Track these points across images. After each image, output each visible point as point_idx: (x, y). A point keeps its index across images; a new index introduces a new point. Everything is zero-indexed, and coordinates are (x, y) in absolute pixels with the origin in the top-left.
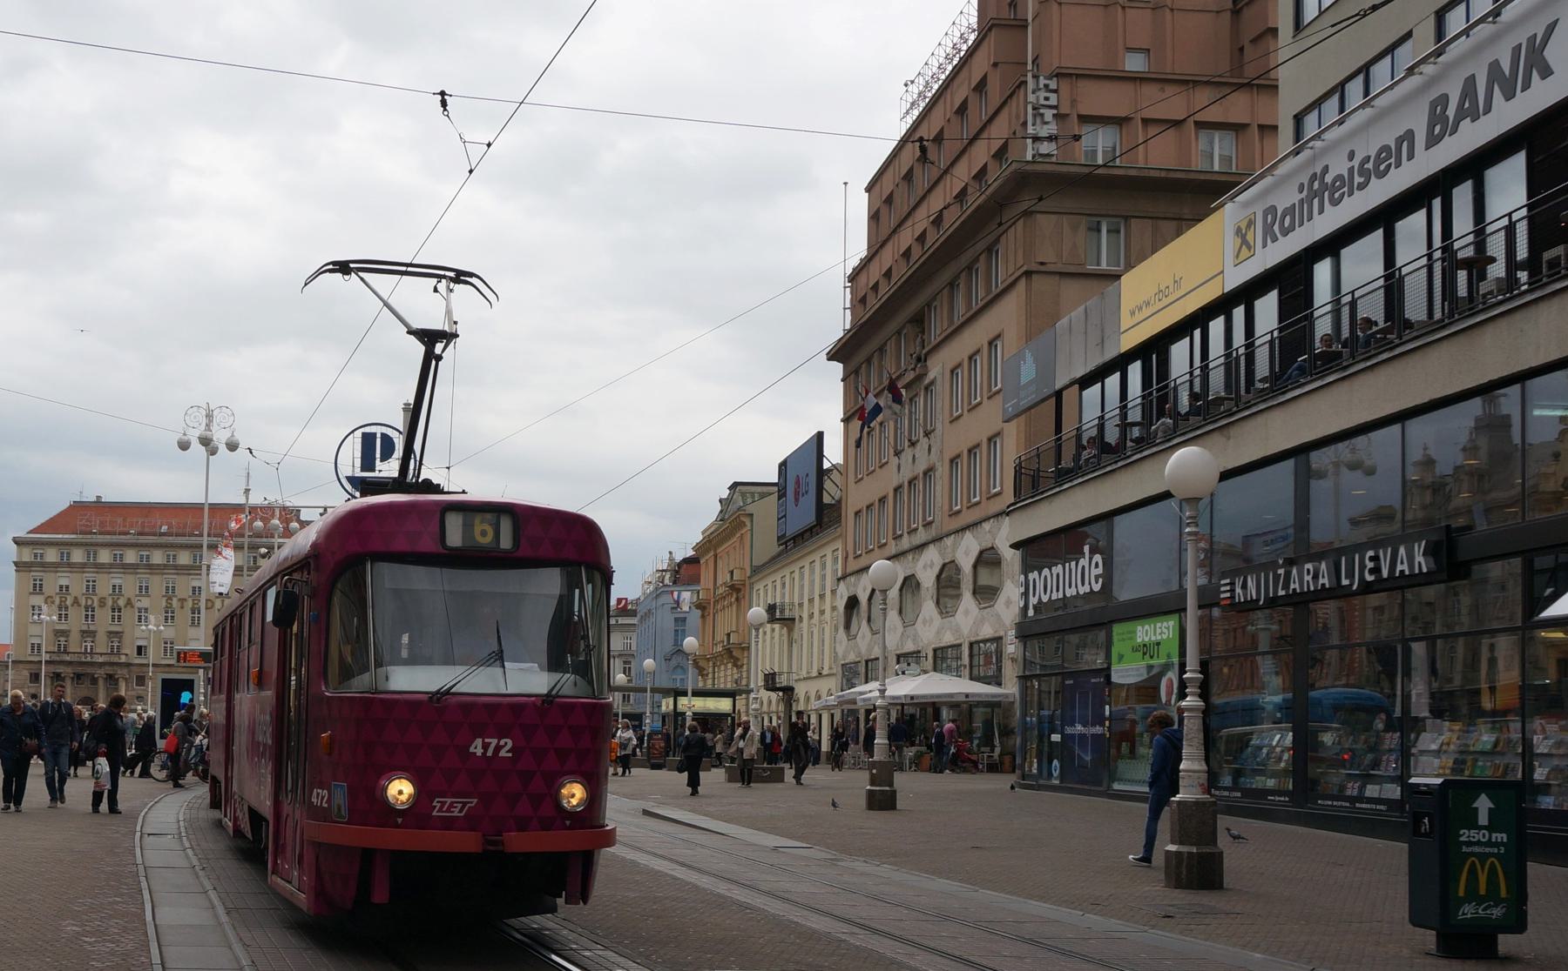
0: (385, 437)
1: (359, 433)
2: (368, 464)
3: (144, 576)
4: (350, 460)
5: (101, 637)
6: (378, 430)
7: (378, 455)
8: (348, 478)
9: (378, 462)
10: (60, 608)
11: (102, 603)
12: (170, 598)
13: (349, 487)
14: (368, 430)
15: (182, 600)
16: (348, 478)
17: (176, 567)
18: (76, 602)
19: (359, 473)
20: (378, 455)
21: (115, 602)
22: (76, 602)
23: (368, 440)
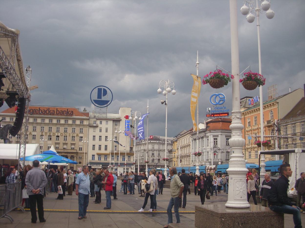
0: (104, 89)
1: (97, 88)
2: (99, 96)
3: (35, 125)
4: (95, 96)
7: (102, 95)
9: (102, 97)
10: (65, 136)
12: (42, 132)
14: (100, 87)
15: (46, 133)
16: (93, 100)
17: (45, 124)
20: (102, 95)
21: (26, 133)
23: (100, 90)
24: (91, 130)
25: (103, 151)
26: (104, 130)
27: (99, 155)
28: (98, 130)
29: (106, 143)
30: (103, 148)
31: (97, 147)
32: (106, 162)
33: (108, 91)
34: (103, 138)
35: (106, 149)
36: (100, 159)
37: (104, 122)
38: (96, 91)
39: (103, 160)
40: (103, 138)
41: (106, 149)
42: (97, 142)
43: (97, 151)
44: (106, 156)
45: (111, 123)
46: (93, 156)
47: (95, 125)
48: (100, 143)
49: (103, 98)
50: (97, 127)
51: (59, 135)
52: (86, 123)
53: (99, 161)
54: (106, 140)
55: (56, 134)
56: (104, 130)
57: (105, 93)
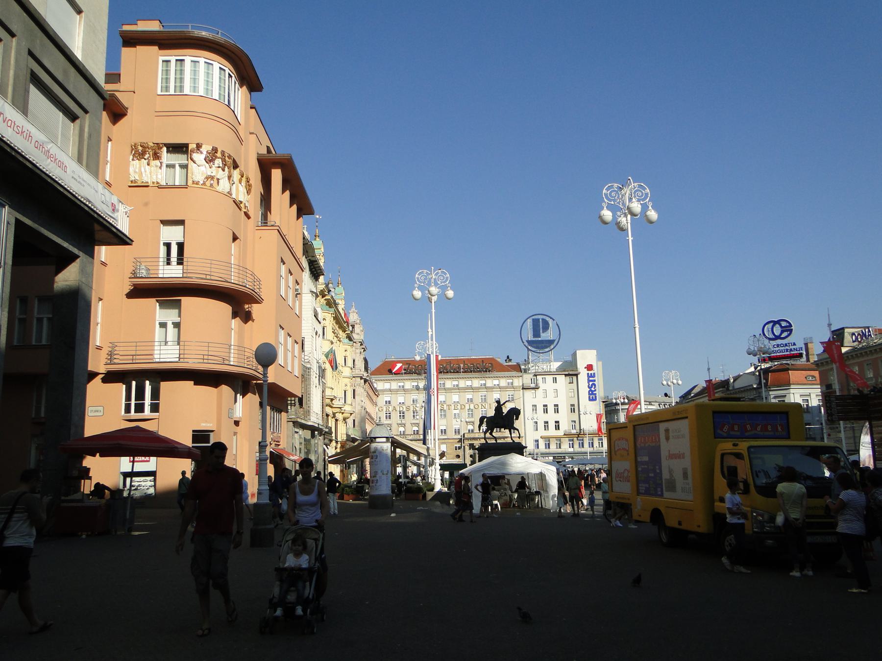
0: (543, 319)
2: (536, 334)
5: (408, 425)
6: (540, 317)
8: (528, 341)
9: (542, 334)
11: (408, 409)
13: (526, 344)
16: (528, 341)
18: (394, 408)
19: (531, 338)
22: (394, 408)
23: (536, 323)
24: (529, 394)
25: (552, 432)
26: (551, 393)
27: (548, 440)
28: (539, 392)
29: (557, 417)
30: (552, 425)
31: (541, 425)
32: (559, 450)
33: (550, 322)
34: (551, 409)
35: (557, 428)
36: (548, 446)
37: (549, 379)
38: (529, 322)
39: (553, 448)
40: (551, 409)
41: (557, 428)
42: (541, 417)
43: (541, 432)
44: (559, 439)
45: (561, 379)
46: (537, 441)
47: (533, 385)
48: (546, 417)
49: (544, 336)
50: (536, 388)
51: (472, 407)
52: (517, 382)
53: (547, 450)
54: (557, 411)
55: (467, 407)
56: (551, 393)
57: (546, 327)
